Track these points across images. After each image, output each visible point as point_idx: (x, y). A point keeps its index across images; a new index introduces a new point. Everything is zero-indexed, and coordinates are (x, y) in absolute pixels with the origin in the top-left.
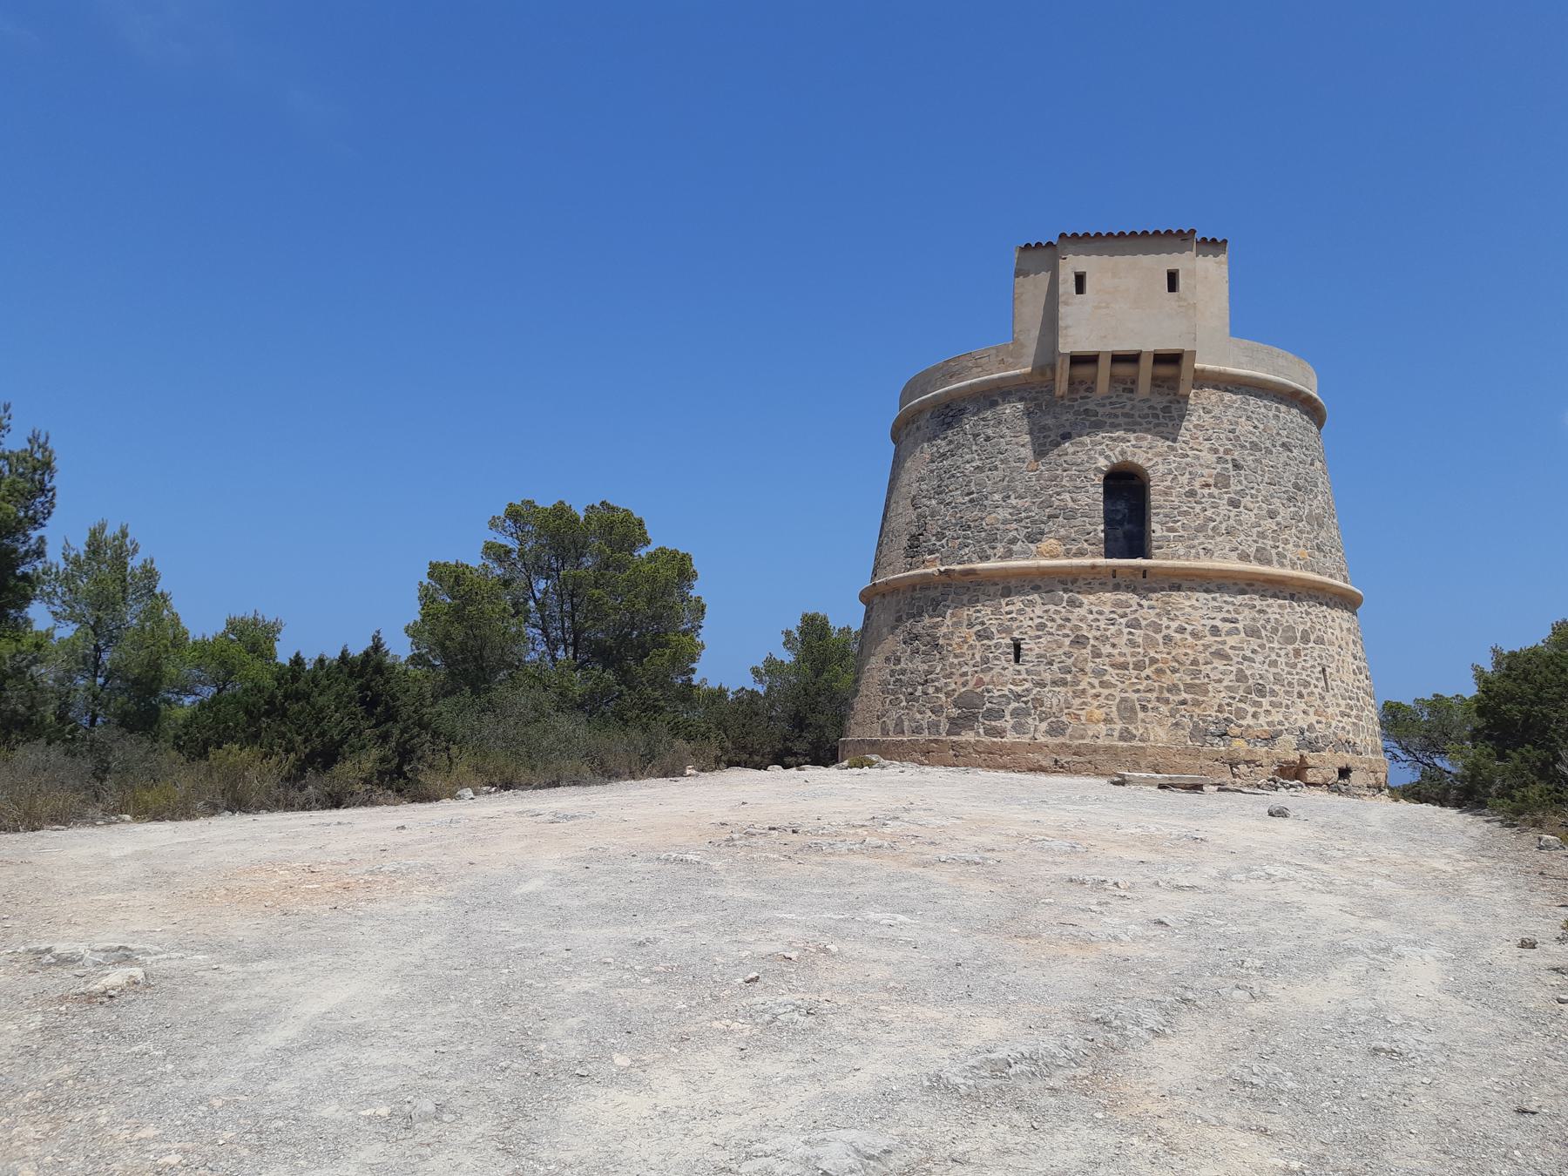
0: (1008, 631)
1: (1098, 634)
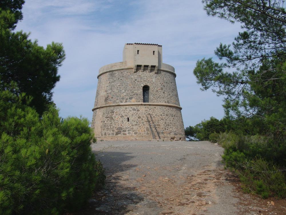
0: (127, 116)
1: (142, 116)
